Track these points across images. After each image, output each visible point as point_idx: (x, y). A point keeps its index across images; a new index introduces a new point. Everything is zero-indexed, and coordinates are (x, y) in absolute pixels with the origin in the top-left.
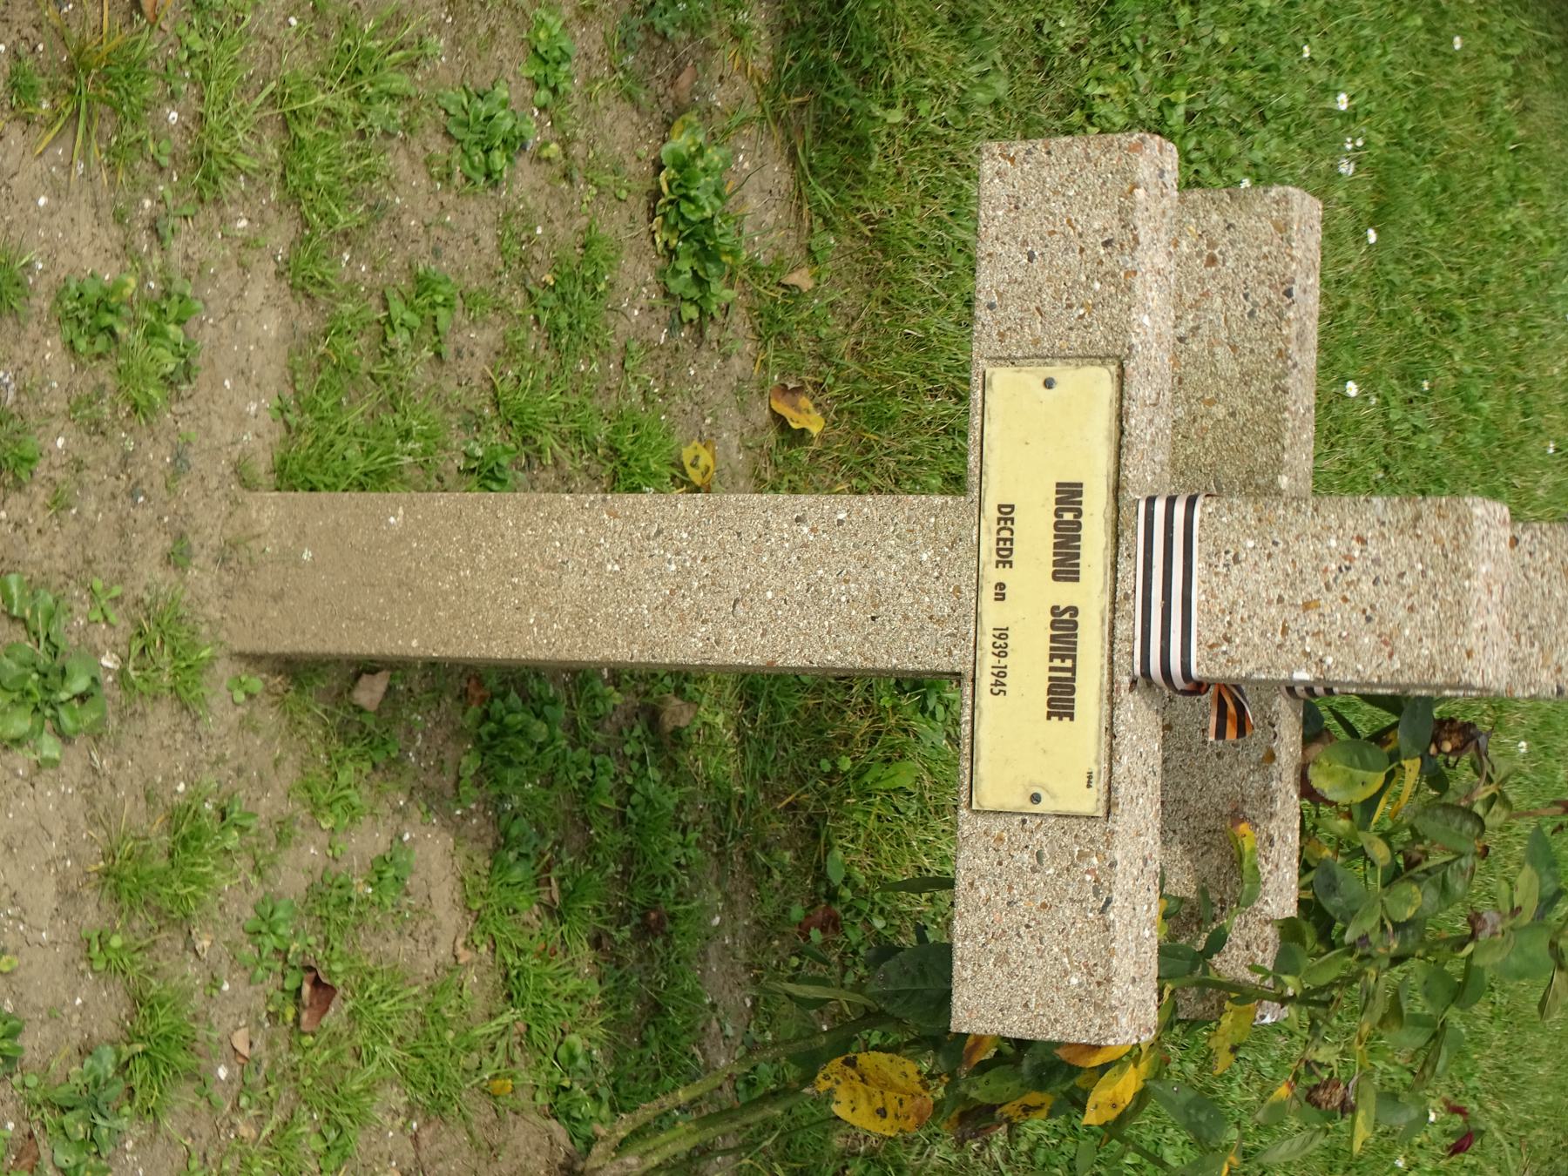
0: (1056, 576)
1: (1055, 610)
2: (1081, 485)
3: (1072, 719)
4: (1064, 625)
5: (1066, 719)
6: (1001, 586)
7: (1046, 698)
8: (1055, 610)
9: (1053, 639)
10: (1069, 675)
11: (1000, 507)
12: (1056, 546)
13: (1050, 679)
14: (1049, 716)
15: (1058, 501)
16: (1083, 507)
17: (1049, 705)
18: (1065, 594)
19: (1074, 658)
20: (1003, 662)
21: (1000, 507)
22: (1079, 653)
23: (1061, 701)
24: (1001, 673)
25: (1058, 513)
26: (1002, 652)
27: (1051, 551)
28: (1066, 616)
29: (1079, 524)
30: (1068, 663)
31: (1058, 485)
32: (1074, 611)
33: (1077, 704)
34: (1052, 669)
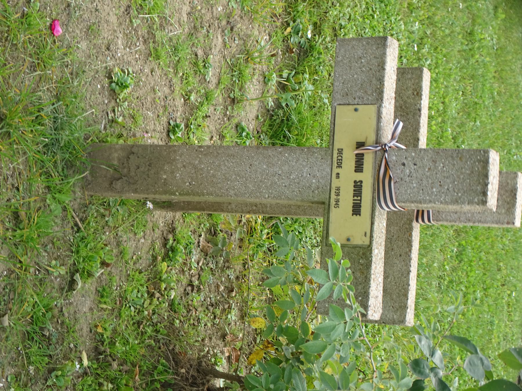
0: (356, 171)
1: (355, 182)
4: (358, 187)
6: (338, 174)
7: (352, 209)
10: (359, 202)
13: (353, 203)
14: (353, 215)
17: (353, 211)
18: (359, 177)
19: (361, 197)
20: (338, 197)
22: (363, 195)
23: (357, 210)
26: (338, 195)
28: (359, 184)
30: (359, 198)
32: (361, 182)
34: (354, 200)
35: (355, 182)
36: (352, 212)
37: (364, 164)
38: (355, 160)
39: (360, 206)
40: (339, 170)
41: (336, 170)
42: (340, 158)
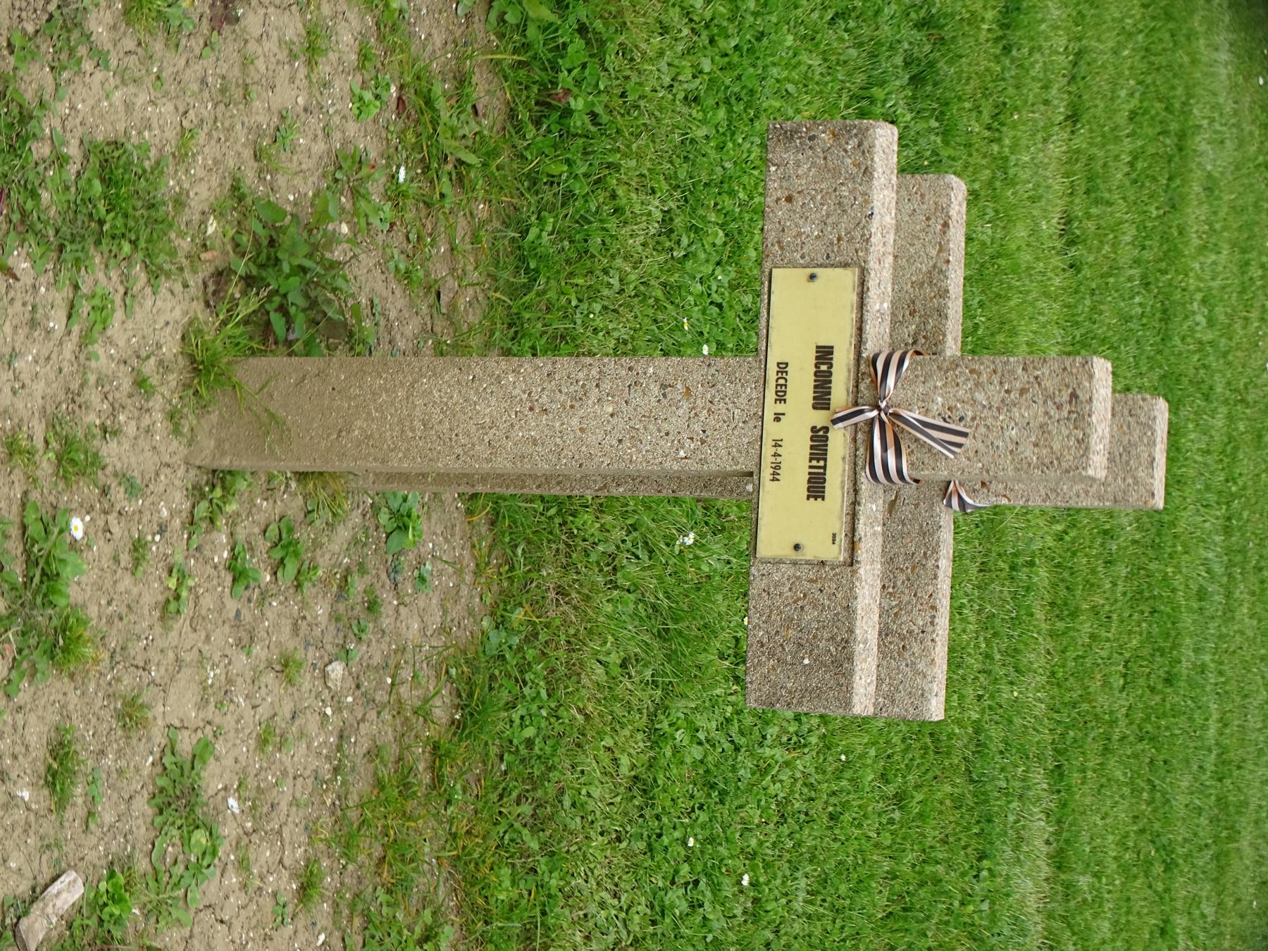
0: (815, 407)
1: (814, 429)
8: (814, 429)
9: (812, 447)
12: (816, 387)
14: (808, 497)
15: (817, 358)
16: (834, 362)
19: (825, 460)
20: (779, 459)
23: (816, 487)
24: (777, 467)
25: (817, 366)
27: (812, 390)
28: (821, 433)
29: (830, 374)
30: (822, 463)
33: (827, 490)
34: (811, 467)
38: (813, 384)
40: (780, 408)
41: (771, 408)
42: (781, 382)
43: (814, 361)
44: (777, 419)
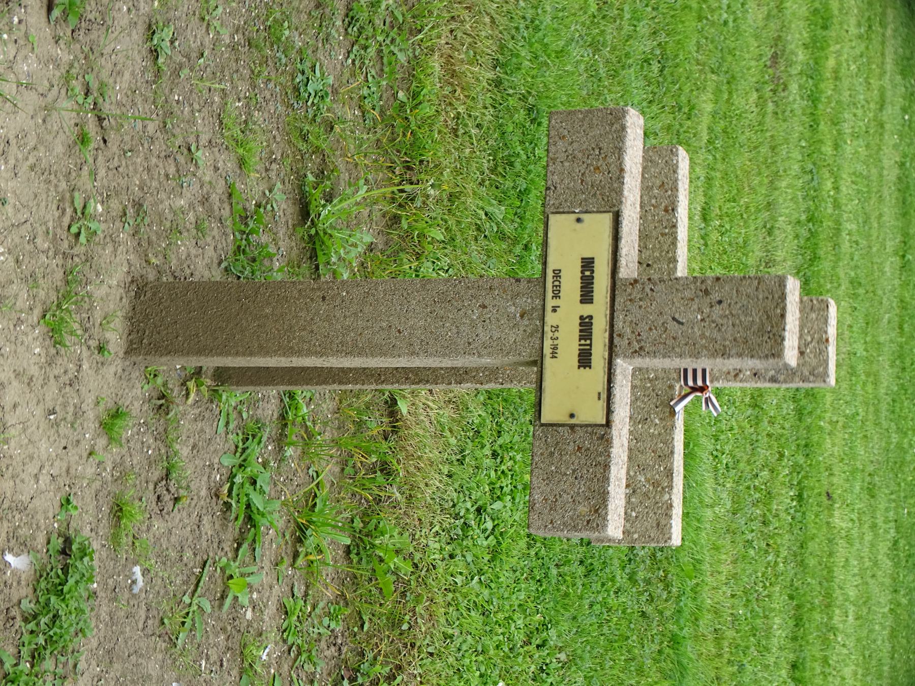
0: (582, 302)
1: (581, 318)
2: (593, 258)
3: (590, 367)
4: (586, 325)
5: (587, 369)
9: (581, 331)
11: (554, 271)
14: (579, 367)
15: (582, 266)
17: (579, 361)
18: (587, 310)
19: (591, 339)
21: (554, 271)
22: (594, 337)
23: (585, 359)
25: (582, 272)
29: (593, 277)
30: (588, 342)
31: (582, 259)
32: (591, 317)
34: (580, 345)
35: (581, 318)
36: (577, 364)
37: (595, 289)
39: (591, 354)
43: (580, 269)
44: (554, 310)
